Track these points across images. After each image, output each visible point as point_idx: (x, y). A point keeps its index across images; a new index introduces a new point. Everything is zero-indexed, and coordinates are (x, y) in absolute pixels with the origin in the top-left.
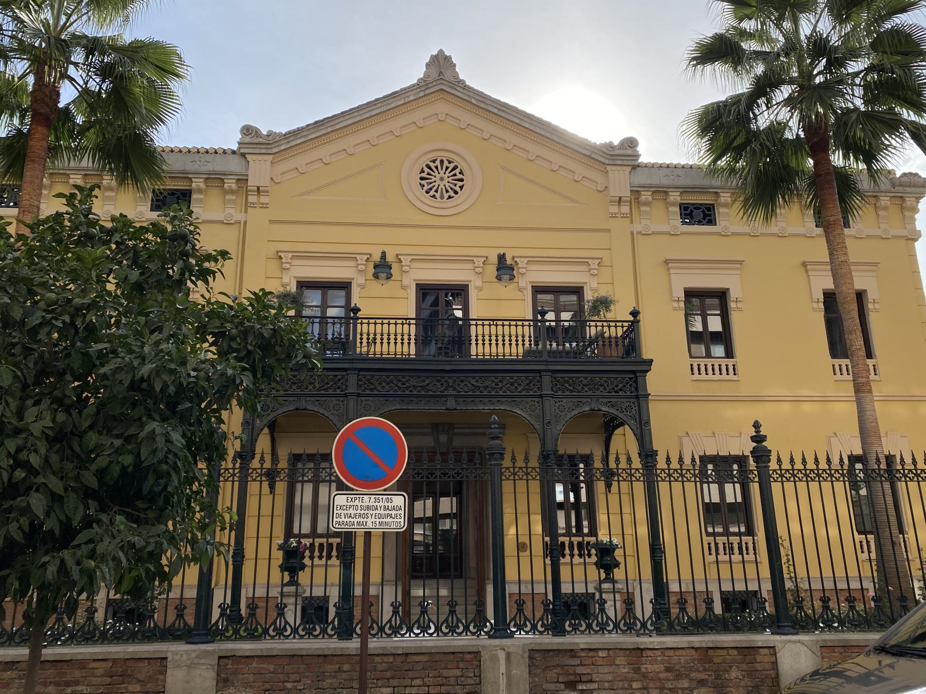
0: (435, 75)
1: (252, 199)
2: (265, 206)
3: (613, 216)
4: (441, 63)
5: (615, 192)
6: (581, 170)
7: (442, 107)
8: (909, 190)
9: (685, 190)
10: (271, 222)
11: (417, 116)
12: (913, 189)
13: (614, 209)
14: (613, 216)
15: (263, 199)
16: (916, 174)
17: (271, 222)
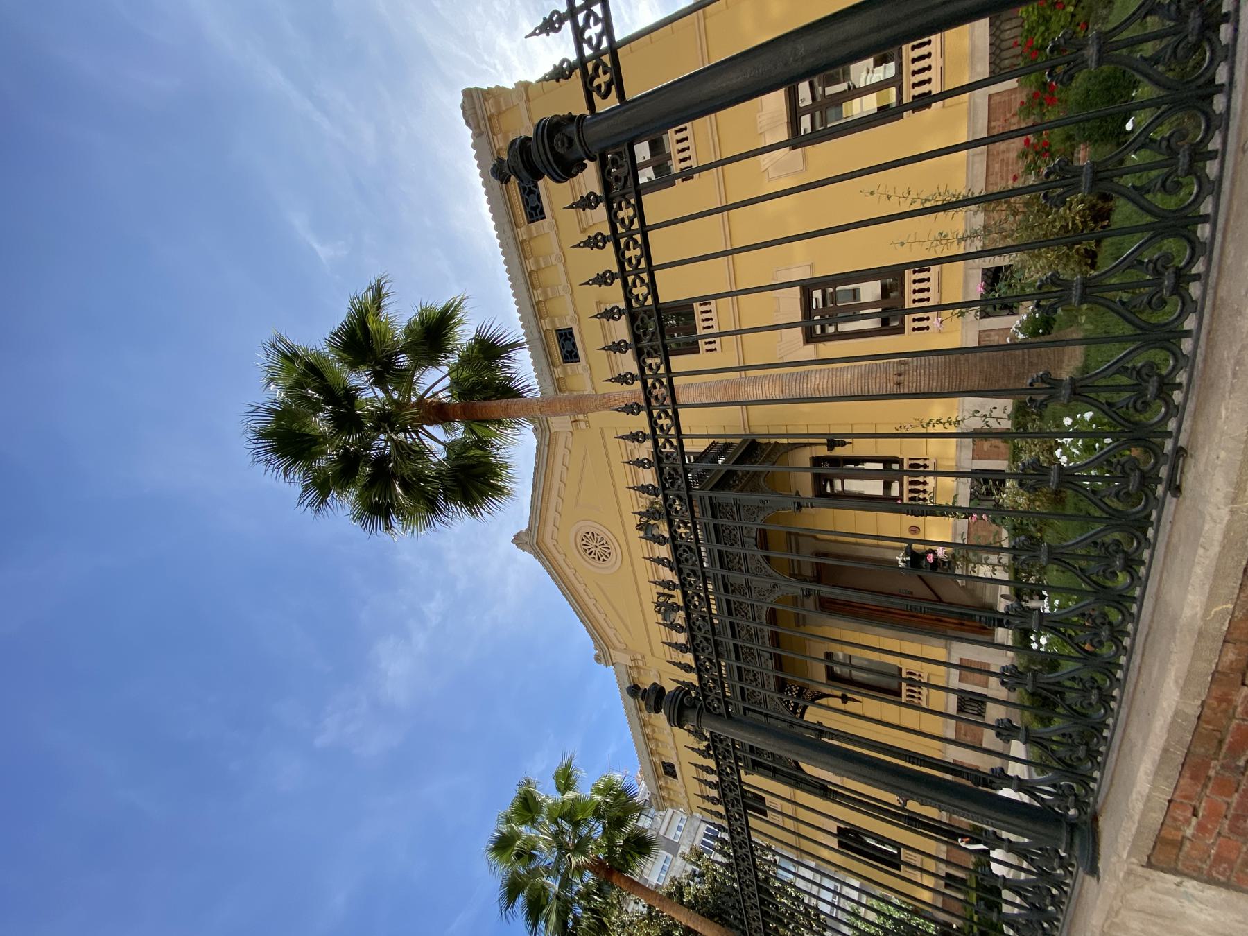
0: (527, 547)
1: (640, 663)
2: (643, 657)
3: (588, 425)
4: (518, 540)
5: (569, 426)
6: (560, 451)
7: (549, 542)
8: (479, 113)
9: (552, 364)
10: (653, 654)
11: (560, 558)
12: (478, 107)
13: (583, 424)
14: (588, 425)
15: (639, 657)
16: (463, 107)
17: (653, 654)
